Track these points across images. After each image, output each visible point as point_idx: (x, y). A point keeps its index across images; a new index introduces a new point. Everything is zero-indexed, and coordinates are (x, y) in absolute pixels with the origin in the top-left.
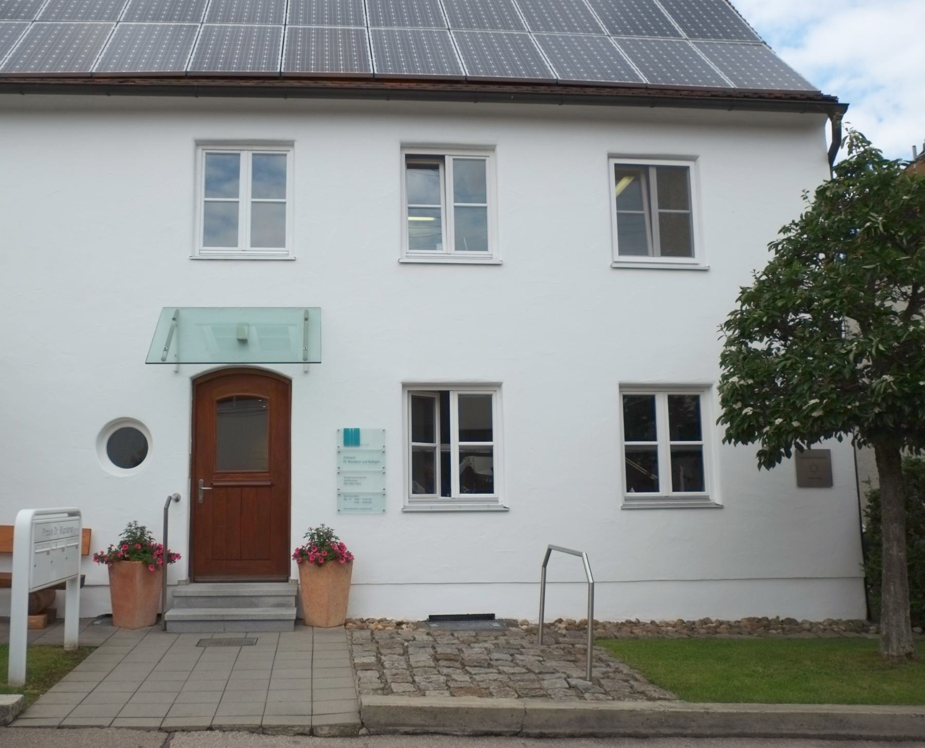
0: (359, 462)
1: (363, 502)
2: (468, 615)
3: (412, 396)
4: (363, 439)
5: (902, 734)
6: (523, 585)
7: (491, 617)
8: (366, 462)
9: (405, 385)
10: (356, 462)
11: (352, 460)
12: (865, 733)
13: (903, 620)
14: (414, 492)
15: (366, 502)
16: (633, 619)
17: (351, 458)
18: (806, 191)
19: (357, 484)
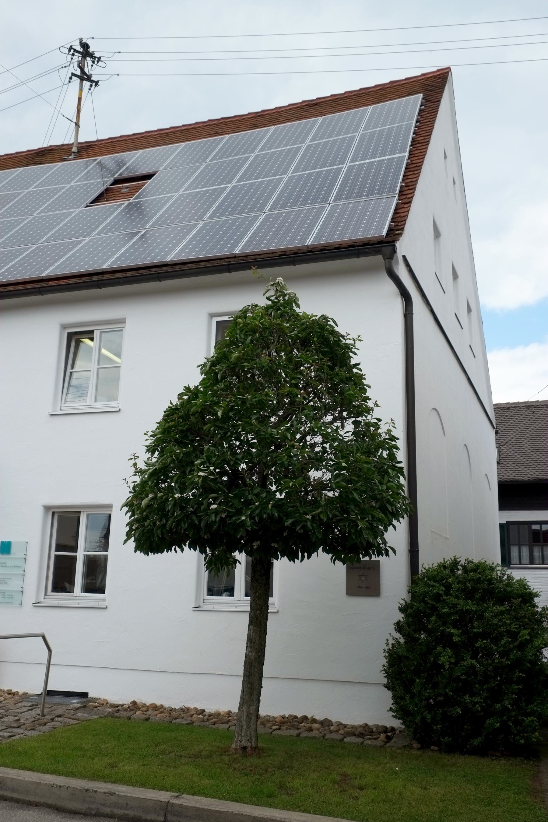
0: (8, 566)
1: (8, 597)
2: (69, 692)
3: (58, 515)
4: (13, 549)
5: (42, 800)
6: (113, 670)
7: (85, 695)
8: (13, 566)
9: (47, 508)
10: (6, 566)
11: (3, 565)
12: (15, 795)
13: (245, 716)
14: (211, 592)
15: (9, 598)
16: (158, 703)
17: (3, 563)
18: (359, 338)
19: (5, 583)
